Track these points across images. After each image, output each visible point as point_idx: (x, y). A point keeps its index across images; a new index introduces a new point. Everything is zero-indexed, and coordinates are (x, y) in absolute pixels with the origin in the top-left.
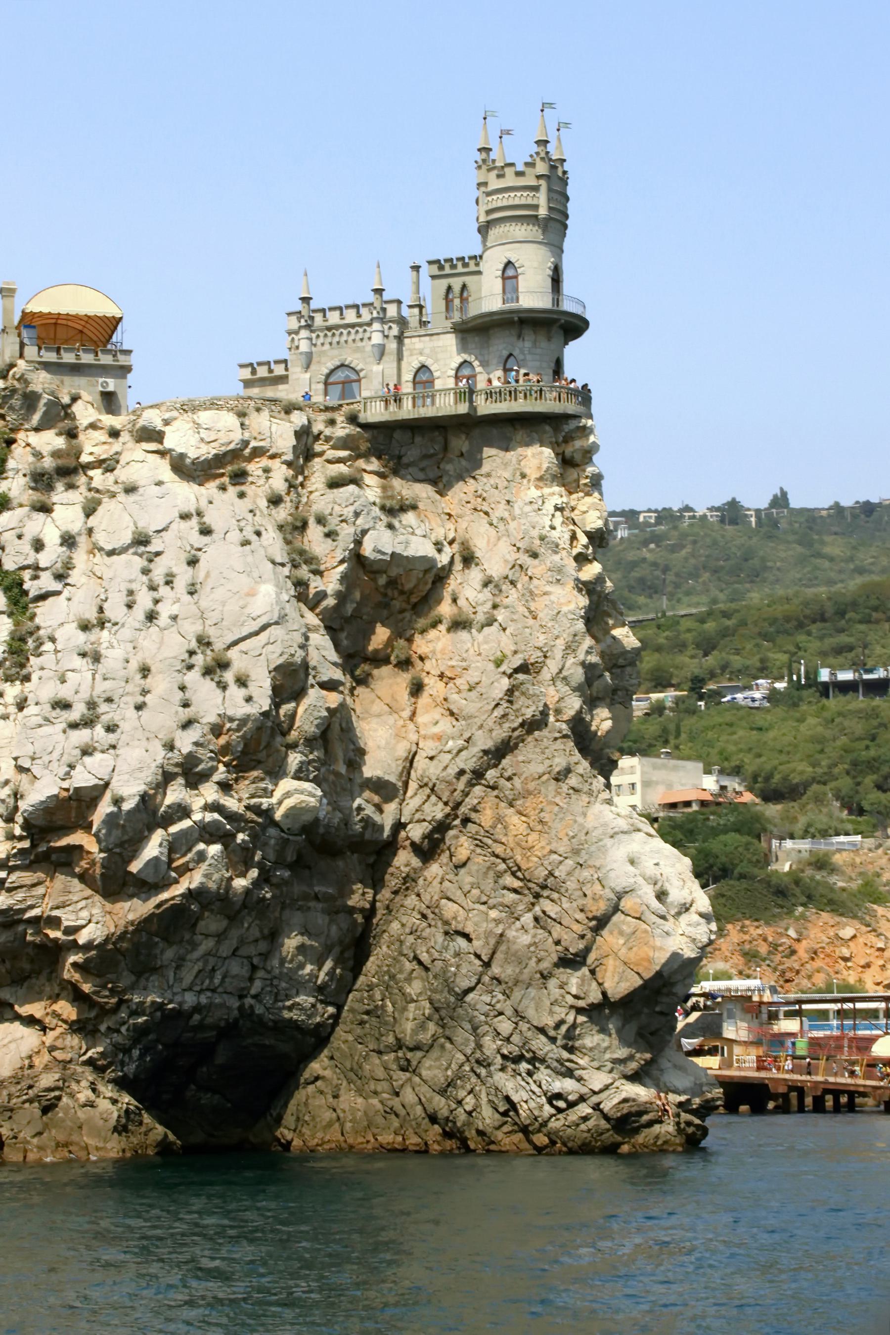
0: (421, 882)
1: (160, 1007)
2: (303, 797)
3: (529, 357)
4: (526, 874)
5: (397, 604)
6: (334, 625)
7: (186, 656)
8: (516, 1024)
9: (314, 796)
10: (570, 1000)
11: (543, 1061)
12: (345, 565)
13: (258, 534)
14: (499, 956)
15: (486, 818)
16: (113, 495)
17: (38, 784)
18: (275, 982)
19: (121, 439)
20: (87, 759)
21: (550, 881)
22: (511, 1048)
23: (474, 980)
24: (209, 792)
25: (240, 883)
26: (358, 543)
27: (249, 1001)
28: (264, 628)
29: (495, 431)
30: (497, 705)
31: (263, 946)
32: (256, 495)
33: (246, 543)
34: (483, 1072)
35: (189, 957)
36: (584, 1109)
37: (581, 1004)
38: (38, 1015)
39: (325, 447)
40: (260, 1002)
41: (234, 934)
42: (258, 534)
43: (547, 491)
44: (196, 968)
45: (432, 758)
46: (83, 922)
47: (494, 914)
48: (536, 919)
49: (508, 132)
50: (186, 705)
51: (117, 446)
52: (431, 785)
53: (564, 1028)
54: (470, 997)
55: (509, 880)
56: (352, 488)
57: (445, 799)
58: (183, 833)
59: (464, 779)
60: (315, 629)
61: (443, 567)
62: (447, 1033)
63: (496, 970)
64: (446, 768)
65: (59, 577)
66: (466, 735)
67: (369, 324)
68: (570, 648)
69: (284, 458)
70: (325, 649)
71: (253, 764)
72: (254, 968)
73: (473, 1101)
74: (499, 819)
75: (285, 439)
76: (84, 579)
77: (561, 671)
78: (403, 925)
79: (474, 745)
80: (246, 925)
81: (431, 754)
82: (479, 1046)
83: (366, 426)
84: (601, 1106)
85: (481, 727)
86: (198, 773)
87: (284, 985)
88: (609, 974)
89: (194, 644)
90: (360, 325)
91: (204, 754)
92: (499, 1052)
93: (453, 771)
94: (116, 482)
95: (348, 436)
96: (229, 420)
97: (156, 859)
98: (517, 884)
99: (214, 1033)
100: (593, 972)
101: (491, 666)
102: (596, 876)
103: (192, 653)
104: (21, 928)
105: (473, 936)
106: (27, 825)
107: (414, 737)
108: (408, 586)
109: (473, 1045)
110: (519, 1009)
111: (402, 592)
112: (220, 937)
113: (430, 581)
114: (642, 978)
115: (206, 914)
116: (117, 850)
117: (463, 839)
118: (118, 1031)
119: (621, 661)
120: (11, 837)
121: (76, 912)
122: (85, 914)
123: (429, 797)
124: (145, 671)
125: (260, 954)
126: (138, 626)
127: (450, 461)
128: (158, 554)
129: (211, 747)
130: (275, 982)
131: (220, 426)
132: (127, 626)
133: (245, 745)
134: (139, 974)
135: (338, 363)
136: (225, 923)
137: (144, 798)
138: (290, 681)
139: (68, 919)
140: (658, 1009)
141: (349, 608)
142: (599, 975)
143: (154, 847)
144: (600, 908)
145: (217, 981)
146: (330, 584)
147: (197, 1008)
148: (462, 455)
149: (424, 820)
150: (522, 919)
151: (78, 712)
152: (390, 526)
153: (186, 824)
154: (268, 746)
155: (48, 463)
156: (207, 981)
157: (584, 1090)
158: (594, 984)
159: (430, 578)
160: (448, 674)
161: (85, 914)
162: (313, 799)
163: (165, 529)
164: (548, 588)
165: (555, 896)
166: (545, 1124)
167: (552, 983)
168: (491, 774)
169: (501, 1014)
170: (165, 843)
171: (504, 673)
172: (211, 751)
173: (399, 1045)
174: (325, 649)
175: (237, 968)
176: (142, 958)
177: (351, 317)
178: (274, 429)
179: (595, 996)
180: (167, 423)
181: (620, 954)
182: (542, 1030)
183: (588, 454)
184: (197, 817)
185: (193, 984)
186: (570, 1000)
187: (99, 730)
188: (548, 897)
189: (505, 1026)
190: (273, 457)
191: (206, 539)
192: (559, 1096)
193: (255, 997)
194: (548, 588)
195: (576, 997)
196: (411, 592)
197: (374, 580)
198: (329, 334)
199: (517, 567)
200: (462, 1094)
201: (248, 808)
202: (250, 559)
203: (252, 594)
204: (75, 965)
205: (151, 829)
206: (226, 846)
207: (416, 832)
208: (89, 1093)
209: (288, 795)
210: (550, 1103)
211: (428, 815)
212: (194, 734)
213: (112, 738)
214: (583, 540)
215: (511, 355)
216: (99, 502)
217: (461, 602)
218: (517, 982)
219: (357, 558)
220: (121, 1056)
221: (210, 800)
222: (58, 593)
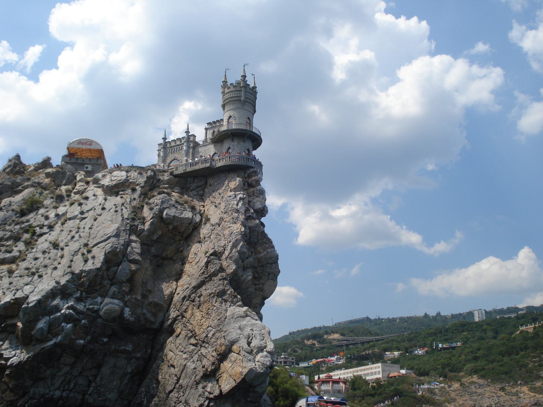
1: (43, 396)
3: (236, 148)
14: (183, 375)
18: (99, 388)
26: (161, 211)
32: (127, 198)
44: (61, 379)
47: (185, 356)
49: (228, 69)
58: (56, 318)
60: (135, 242)
67: (183, 144)
68: (234, 246)
70: (135, 248)
71: (93, 291)
80: (85, 361)
83: (176, 176)
86: (67, 294)
87: (102, 390)
90: (180, 145)
95: (168, 180)
97: (42, 328)
105: (176, 366)
108: (182, 230)
111: (179, 232)
112: (73, 366)
113: (191, 228)
115: (64, 355)
116: (27, 325)
119: (270, 261)
125: (93, 375)
129: (75, 283)
133: (90, 283)
140: (249, 399)
141: (155, 237)
142: (220, 382)
143: (41, 324)
145: (72, 386)
146: (147, 226)
147: (61, 398)
154: (101, 283)
156: (67, 386)
161: (13, 353)
162: (117, 307)
164: (231, 225)
165: (207, 345)
167: (200, 386)
172: (74, 285)
174: (135, 248)
175: (81, 380)
177: (178, 143)
179: (217, 392)
186: (207, 394)
188: (204, 347)
193: (90, 394)
194: (231, 225)
195: (210, 393)
197: (168, 227)
201: (88, 309)
205: (43, 316)
206: (75, 326)
209: (107, 304)
219: (159, 217)
222: (46, 233)
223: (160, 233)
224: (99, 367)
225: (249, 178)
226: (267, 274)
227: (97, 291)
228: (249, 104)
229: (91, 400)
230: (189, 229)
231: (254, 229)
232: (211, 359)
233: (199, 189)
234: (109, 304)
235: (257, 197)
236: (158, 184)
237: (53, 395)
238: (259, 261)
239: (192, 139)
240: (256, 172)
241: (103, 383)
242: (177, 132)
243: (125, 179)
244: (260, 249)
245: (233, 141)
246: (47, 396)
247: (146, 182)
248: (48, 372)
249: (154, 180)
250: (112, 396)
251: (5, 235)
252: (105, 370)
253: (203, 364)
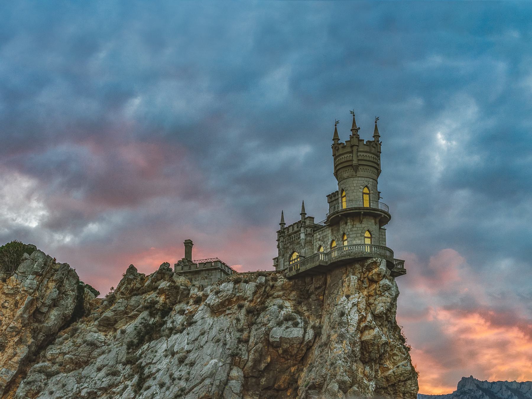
26: (267, 333)
39: (274, 292)
61: (310, 341)
75: (250, 291)
111: (291, 356)
141: (263, 366)
194: (336, 345)
196: (296, 355)
197: (277, 351)
214: (369, 318)
223: (269, 359)
225: (369, 271)
226: (401, 395)
228: (365, 167)
230: (302, 350)
231: (372, 342)
233: (319, 291)
235: (381, 295)
236: (272, 292)
238: (387, 380)
239: (308, 222)
240: (375, 263)
242: (292, 217)
243: (232, 294)
244: (388, 364)
247: (255, 293)
249: (266, 288)
251: (116, 380)
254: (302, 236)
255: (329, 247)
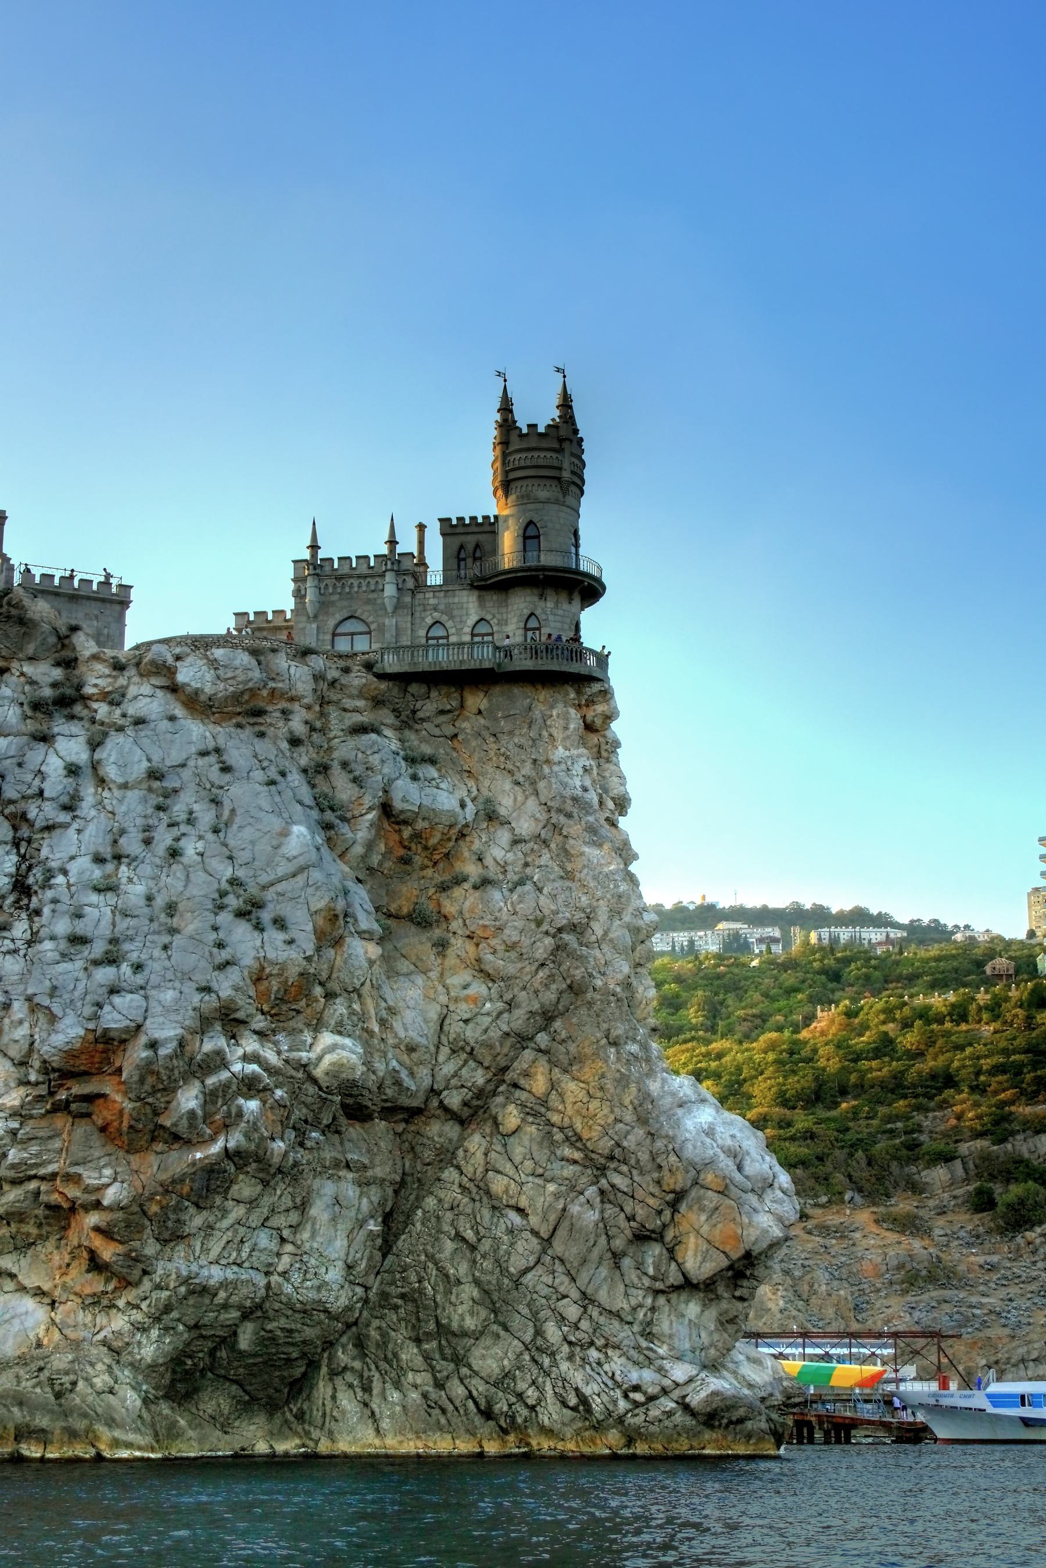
0: (460, 1153)
2: (345, 1053)
3: (551, 618)
4: (589, 1144)
5: (418, 860)
6: (368, 873)
7: (216, 896)
8: (585, 1307)
9: (353, 1052)
10: (647, 1282)
11: (616, 1347)
12: (374, 812)
13: (283, 774)
14: (562, 1233)
15: (539, 1084)
16: (121, 729)
17: (60, 1026)
18: (305, 1258)
19: (126, 673)
20: (117, 1000)
21: (617, 1152)
22: (580, 1335)
23: (532, 1260)
24: (250, 1044)
25: (279, 1146)
27: (275, 1279)
28: (302, 869)
29: (516, 691)
30: (543, 965)
31: (294, 1217)
32: (276, 737)
33: (272, 783)
34: (546, 1361)
35: (218, 1225)
36: (668, 1404)
37: (659, 1285)
38: (46, 1287)
40: (288, 1280)
41: (267, 1201)
42: (283, 774)
43: (575, 752)
44: (225, 1239)
45: (466, 1021)
46: (105, 1180)
47: (551, 1187)
48: (602, 1192)
50: (220, 945)
51: (122, 681)
52: (468, 1049)
53: (641, 1314)
54: (529, 1278)
55: (567, 1152)
56: (374, 736)
57: (486, 1064)
59: (508, 1043)
61: (466, 825)
62: (501, 1318)
63: (558, 1247)
64: (486, 1031)
65: (67, 808)
66: (508, 997)
69: (306, 701)
72: (283, 1240)
73: (536, 1394)
74: (553, 1085)
76: (93, 813)
77: (606, 933)
78: (440, 1201)
79: (518, 1006)
80: (278, 1192)
81: (466, 1016)
82: (539, 1332)
84: (687, 1400)
85: (524, 988)
88: (690, 1253)
89: (225, 886)
91: (241, 1001)
92: (565, 1339)
93: (495, 1034)
94: (124, 715)
96: (243, 658)
97: (192, 1113)
98: (577, 1155)
99: (238, 1314)
100: (671, 1251)
101: (533, 926)
102: (671, 1147)
103: (223, 894)
104: (33, 1185)
106: (46, 1068)
107: (443, 999)
108: (433, 841)
109: (531, 1331)
110: (589, 1291)
111: (426, 848)
114: (727, 1256)
117: (511, 1108)
118: (138, 1307)
120: (24, 1083)
121: (100, 1169)
122: (108, 1172)
123: (466, 1062)
124: (171, 909)
126: (158, 861)
127: (467, 719)
128: (176, 791)
130: (305, 1258)
131: (237, 663)
132: (147, 861)
134: (164, 1242)
135: (346, 615)
136: (260, 1187)
137: (182, 1043)
138: (332, 930)
139: (90, 1178)
140: (737, 1294)
143: (189, 1098)
144: (679, 1181)
145: (244, 1255)
147: (224, 1284)
148: (480, 712)
149: (463, 1086)
150: (587, 1193)
151: (98, 949)
152: (414, 778)
153: (224, 1075)
155: (47, 692)
157: (667, 1382)
158: (673, 1265)
159: (454, 832)
160: (479, 932)
163: (183, 765)
165: (624, 1168)
166: (621, 1420)
167: (627, 1262)
168: (542, 1039)
169: (565, 1297)
170: (201, 1096)
171: (547, 933)
173: (443, 1330)
176: (170, 1224)
178: (292, 670)
179: (674, 1277)
180: (178, 658)
181: (702, 1231)
182: (617, 1315)
183: (609, 717)
184: (237, 1067)
185: (220, 1256)
186: (647, 1282)
187: (125, 968)
188: (615, 1170)
189: (572, 1312)
190: (292, 699)
191: (227, 777)
192: (636, 1388)
193: (284, 1274)
198: (339, 585)
199: (549, 826)
200: (521, 1386)
201: (287, 1061)
202: (277, 799)
203: (285, 833)
204: (97, 1229)
207: (454, 1100)
208: (106, 1377)
210: (626, 1396)
211: (466, 1080)
212: (234, 975)
213: (139, 979)
215: (532, 614)
216: (106, 734)
217: (488, 861)
218: (584, 1261)
220: (138, 1336)
221: (249, 1049)
222: (65, 826)
224: (303, 1207)
227: (298, 1012)
229: (288, 1289)
232: (651, 1201)
234: (333, 1051)
237: (210, 1277)
241: (315, 1245)
245: (542, 596)
246: (197, 1281)
248: (198, 1221)
250: (334, 1274)
252: (319, 1211)
253: (628, 1209)
254: (390, 590)
255: (468, 630)
